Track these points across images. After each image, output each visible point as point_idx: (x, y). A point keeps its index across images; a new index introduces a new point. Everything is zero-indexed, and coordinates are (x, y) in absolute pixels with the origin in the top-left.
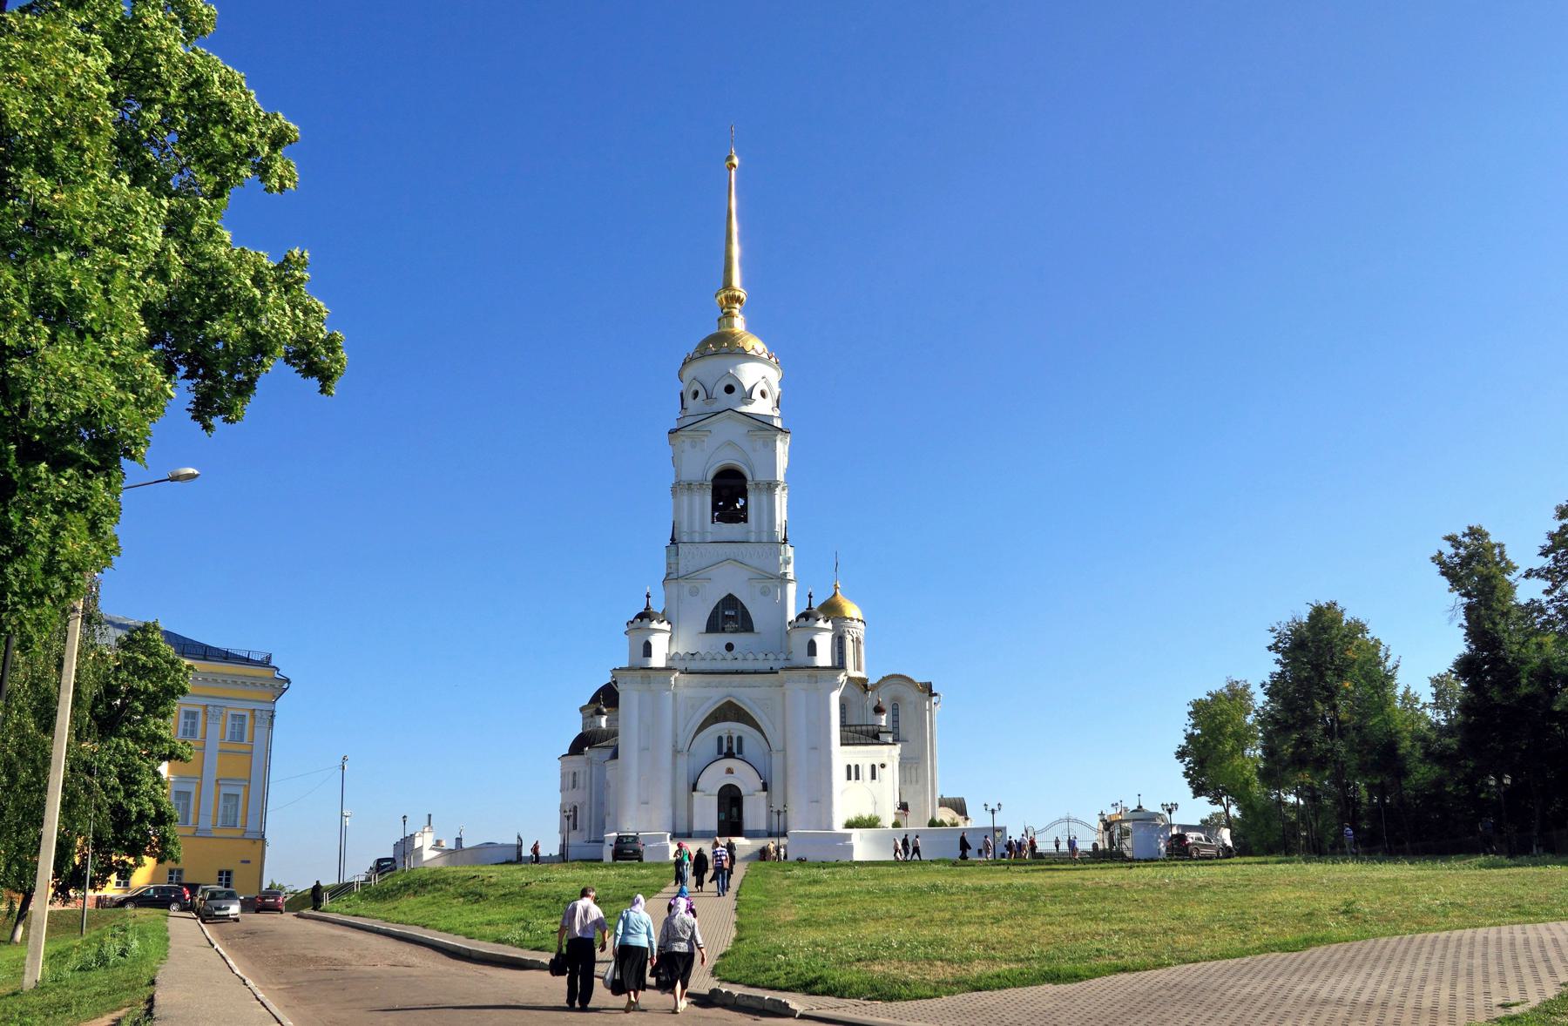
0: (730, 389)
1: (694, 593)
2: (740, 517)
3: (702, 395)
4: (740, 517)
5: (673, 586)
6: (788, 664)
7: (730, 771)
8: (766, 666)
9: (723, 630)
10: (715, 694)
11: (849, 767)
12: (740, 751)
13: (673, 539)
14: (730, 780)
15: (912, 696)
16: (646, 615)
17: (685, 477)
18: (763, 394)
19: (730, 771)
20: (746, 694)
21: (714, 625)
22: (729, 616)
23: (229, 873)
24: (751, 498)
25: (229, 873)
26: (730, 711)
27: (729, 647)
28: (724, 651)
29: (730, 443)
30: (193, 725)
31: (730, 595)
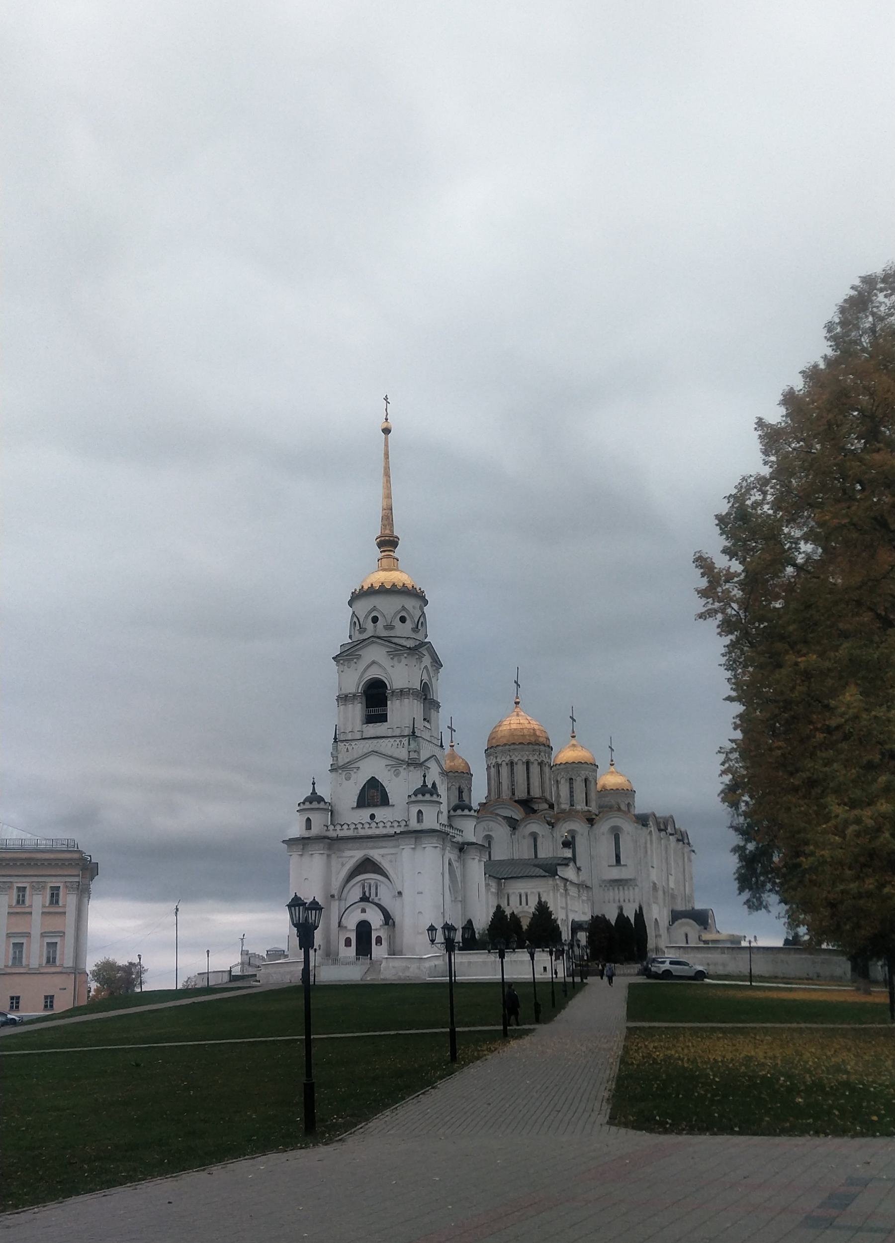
0: (375, 620)
1: (348, 779)
2: (383, 718)
3: (358, 627)
4: (383, 718)
5: (334, 774)
6: (406, 829)
7: (363, 911)
8: (392, 831)
9: (369, 805)
10: (354, 855)
11: (520, 896)
12: (377, 895)
13: (335, 738)
14: (363, 917)
15: (628, 828)
16: (314, 798)
17: (344, 692)
18: (403, 620)
19: (363, 911)
20: (376, 854)
21: (363, 801)
22: (373, 795)
23: (52, 997)
24: (389, 702)
25: (52, 997)
26: (367, 866)
27: (372, 817)
28: (369, 820)
29: (374, 662)
30: (24, 896)
31: (373, 777)
